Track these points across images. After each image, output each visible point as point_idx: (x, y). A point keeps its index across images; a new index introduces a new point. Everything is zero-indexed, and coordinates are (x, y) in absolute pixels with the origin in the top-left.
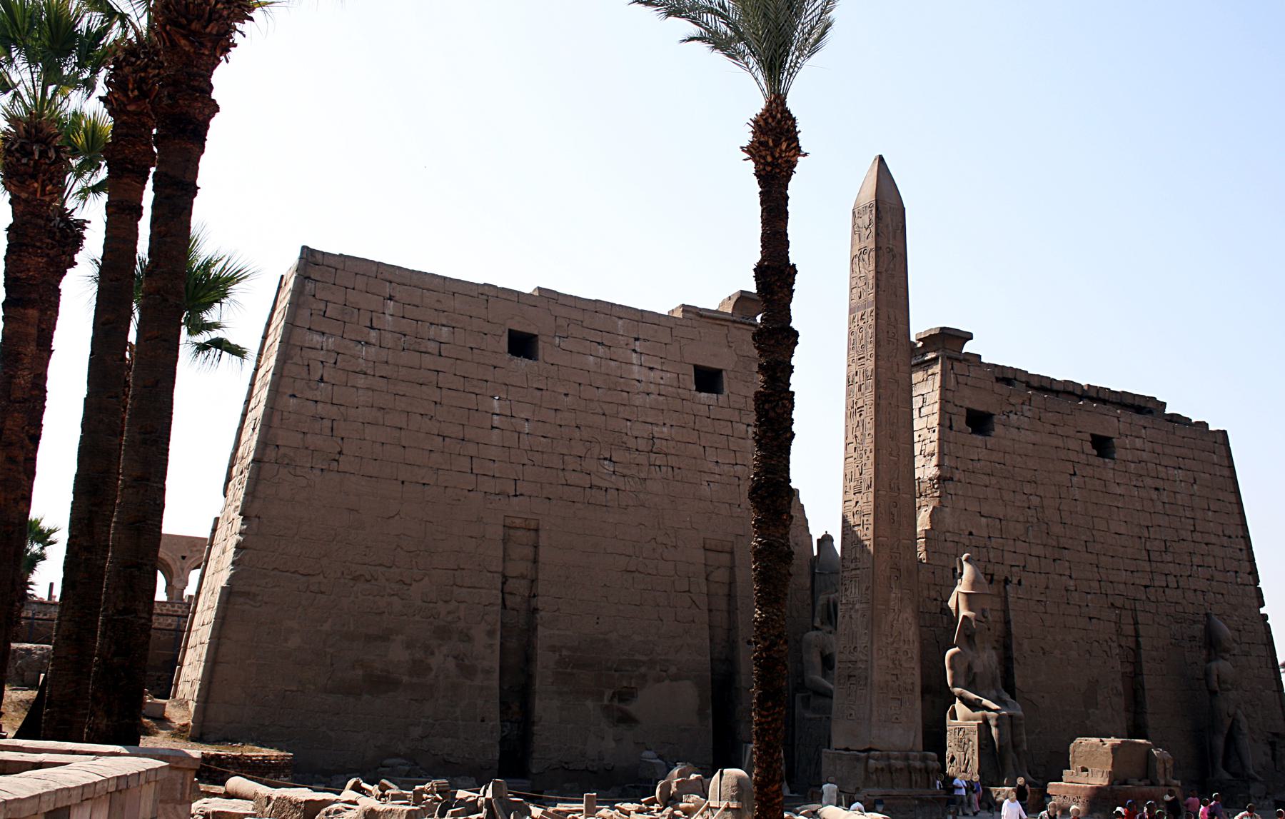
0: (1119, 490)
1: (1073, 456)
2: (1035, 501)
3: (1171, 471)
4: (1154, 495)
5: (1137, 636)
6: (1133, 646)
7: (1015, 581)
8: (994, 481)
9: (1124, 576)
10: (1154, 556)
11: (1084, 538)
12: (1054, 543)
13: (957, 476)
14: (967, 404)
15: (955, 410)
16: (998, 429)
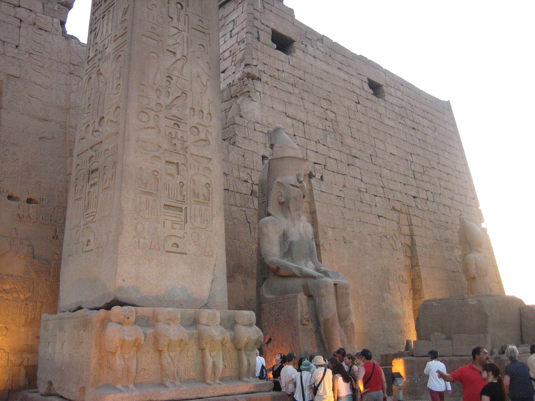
0: (391, 123)
1: (357, 90)
2: (331, 116)
3: (421, 119)
4: (413, 132)
5: (412, 235)
6: (409, 243)
7: (318, 176)
8: (296, 91)
9: (399, 187)
10: (418, 176)
11: (369, 152)
12: (347, 152)
13: (264, 78)
14: (272, 25)
15: (262, 27)
16: (298, 53)
